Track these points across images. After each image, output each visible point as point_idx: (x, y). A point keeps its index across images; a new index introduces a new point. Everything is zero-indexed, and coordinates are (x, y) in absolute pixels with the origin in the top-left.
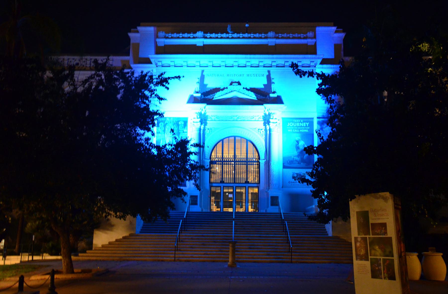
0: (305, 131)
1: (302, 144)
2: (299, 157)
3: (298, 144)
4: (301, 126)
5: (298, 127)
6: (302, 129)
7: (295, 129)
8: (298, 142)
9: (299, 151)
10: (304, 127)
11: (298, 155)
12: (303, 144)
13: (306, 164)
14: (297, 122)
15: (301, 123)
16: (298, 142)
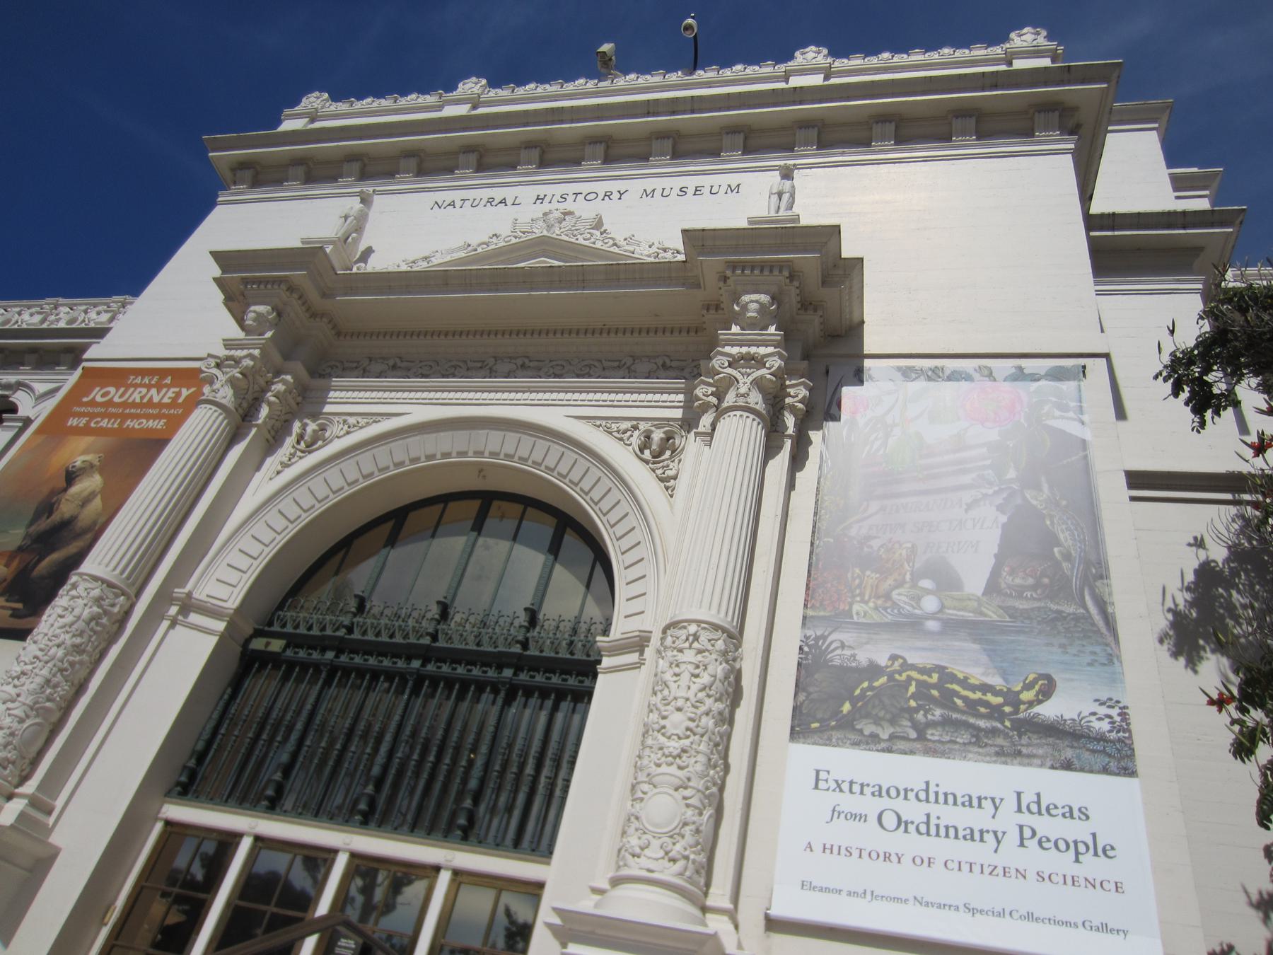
0: (152, 424)
1: (82, 492)
2: (15, 564)
3: (65, 490)
4: (150, 404)
5: (134, 405)
6: (138, 417)
7: (103, 416)
8: (71, 477)
9: (44, 524)
10: (160, 405)
11: (20, 549)
12: (86, 493)
13: (19, 606)
14: (136, 386)
15: (154, 391)
16: (74, 478)
